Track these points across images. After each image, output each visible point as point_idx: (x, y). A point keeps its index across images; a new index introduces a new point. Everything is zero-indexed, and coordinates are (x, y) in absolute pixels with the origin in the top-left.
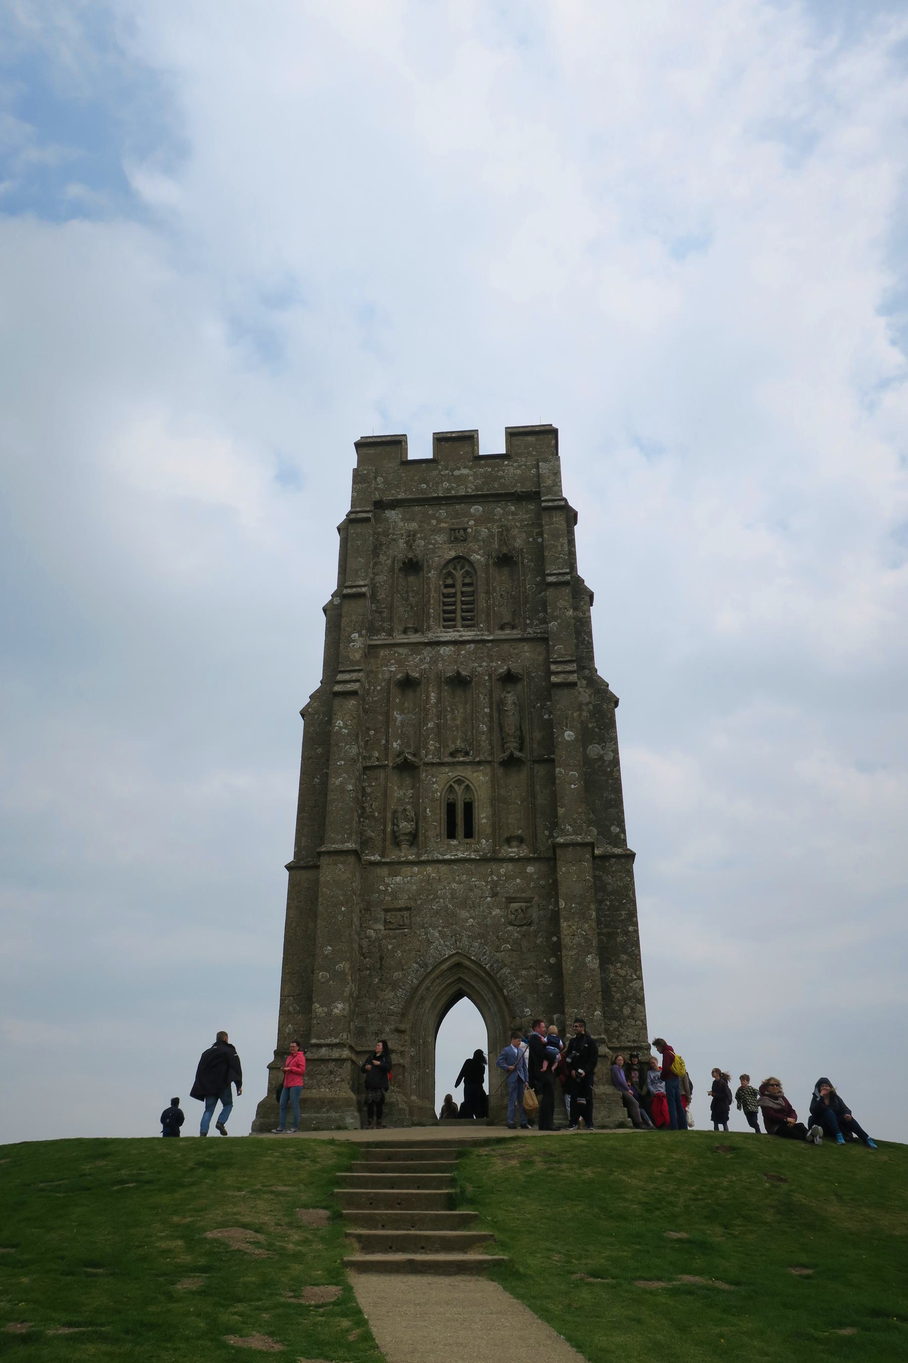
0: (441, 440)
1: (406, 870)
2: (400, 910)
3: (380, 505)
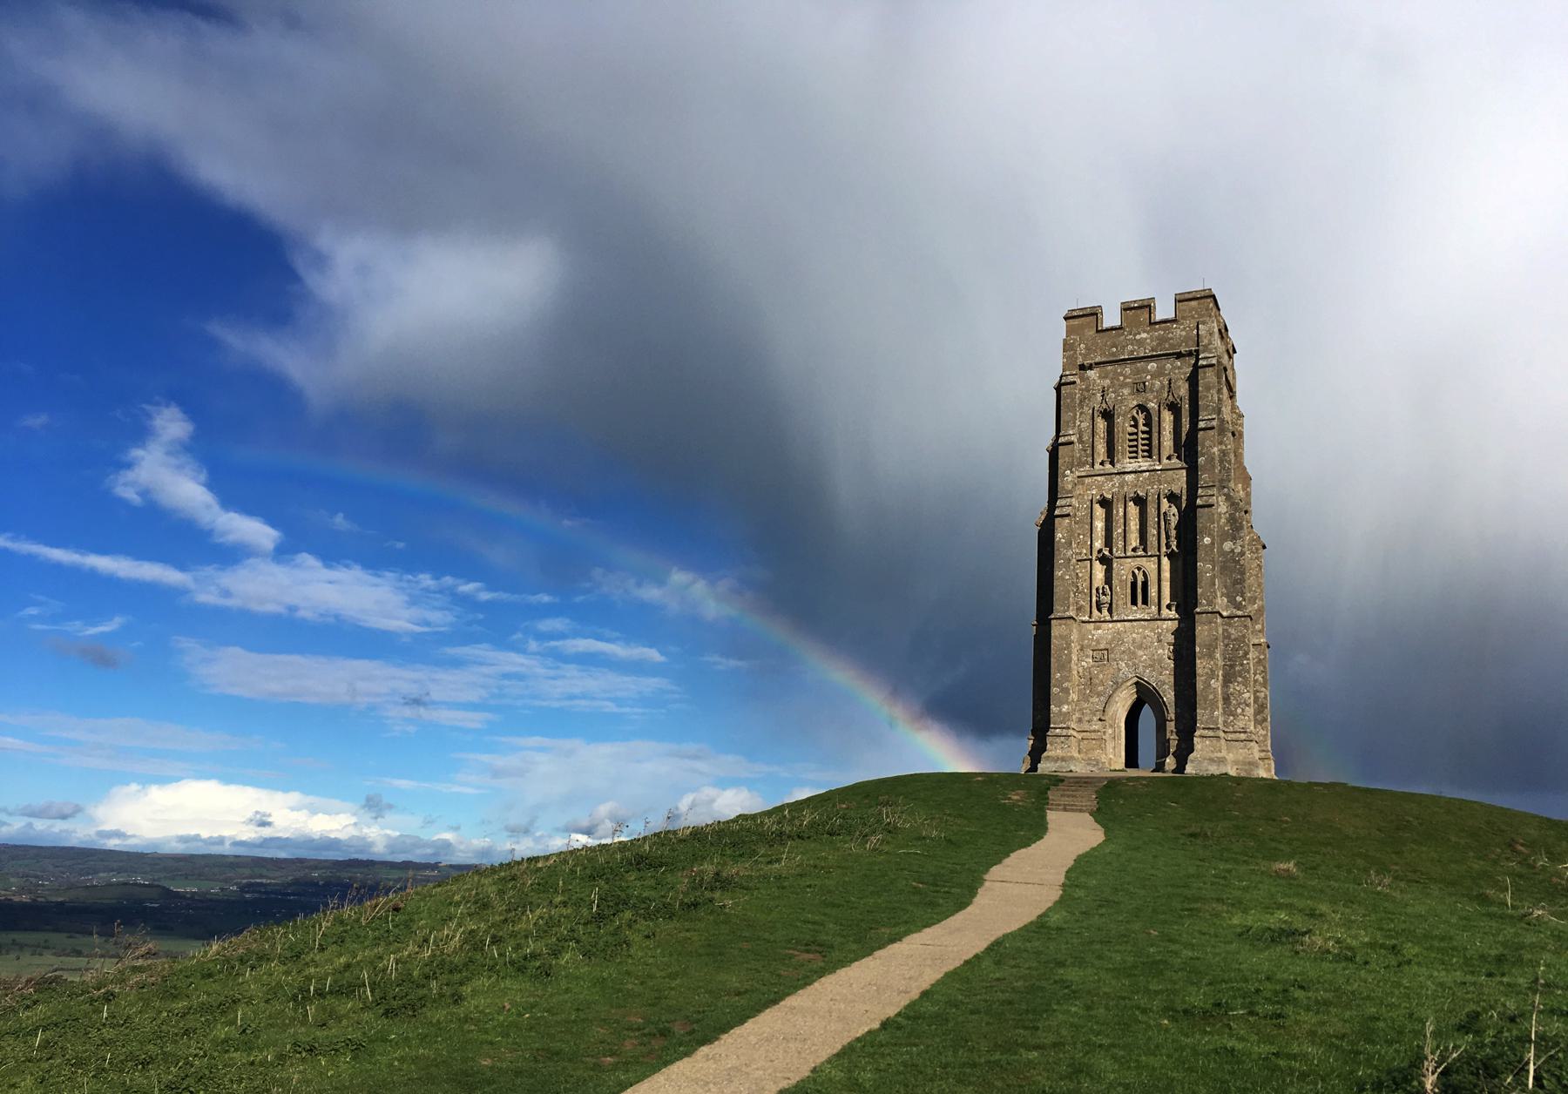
0: (1126, 308)
3: (1082, 367)
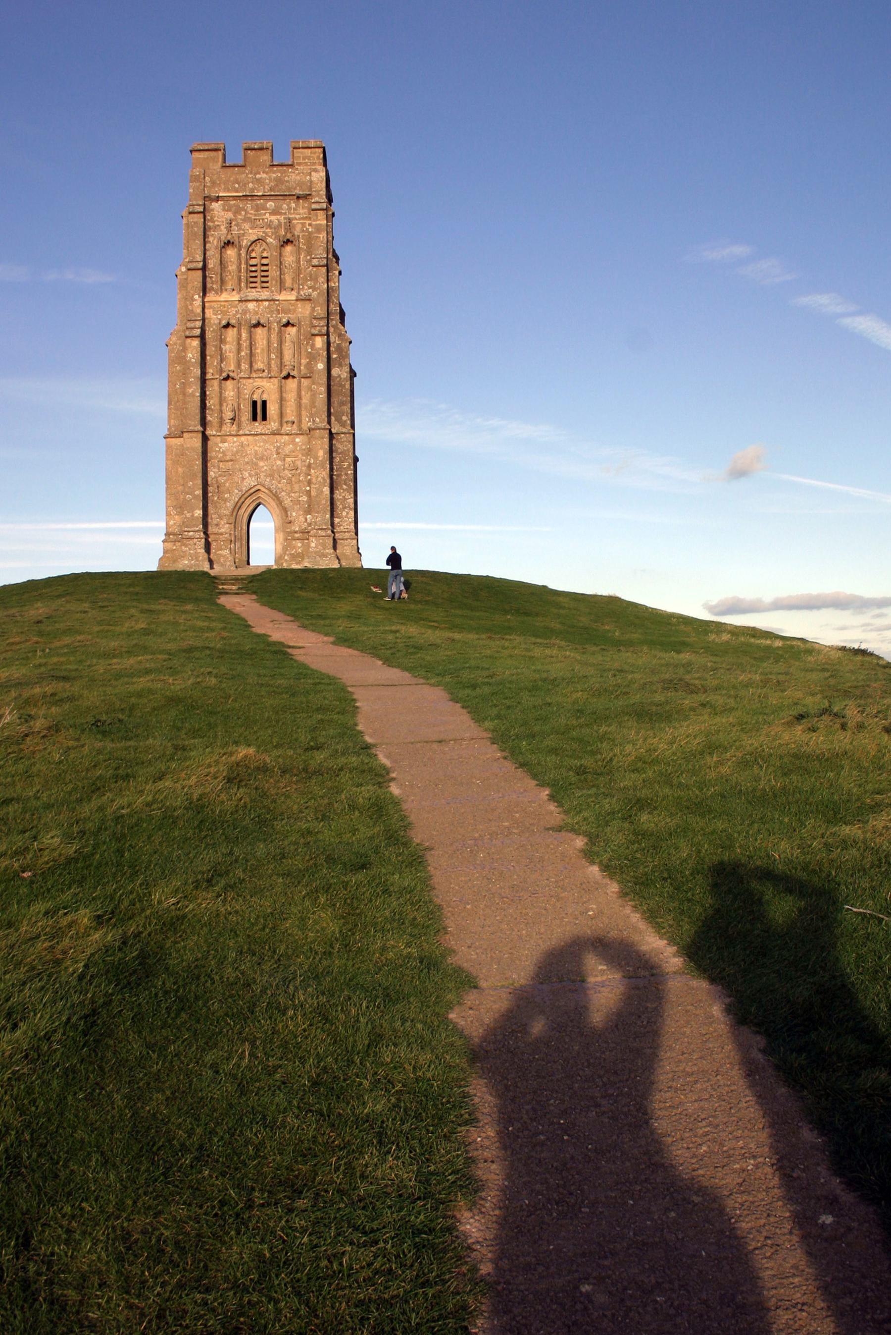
1: (230, 438)
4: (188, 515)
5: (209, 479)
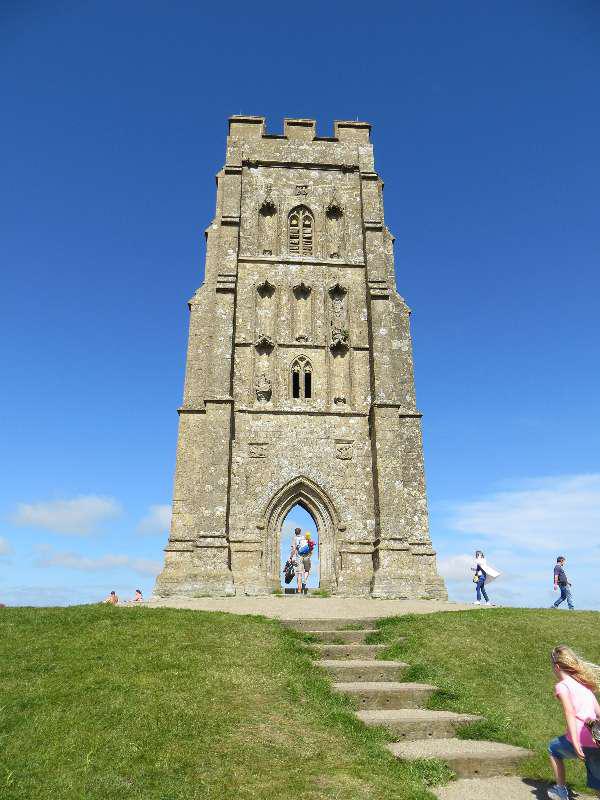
2: (261, 444)
4: (207, 513)
5: (234, 467)
